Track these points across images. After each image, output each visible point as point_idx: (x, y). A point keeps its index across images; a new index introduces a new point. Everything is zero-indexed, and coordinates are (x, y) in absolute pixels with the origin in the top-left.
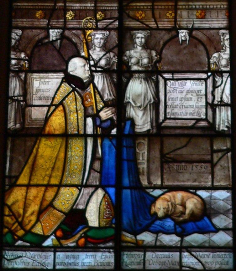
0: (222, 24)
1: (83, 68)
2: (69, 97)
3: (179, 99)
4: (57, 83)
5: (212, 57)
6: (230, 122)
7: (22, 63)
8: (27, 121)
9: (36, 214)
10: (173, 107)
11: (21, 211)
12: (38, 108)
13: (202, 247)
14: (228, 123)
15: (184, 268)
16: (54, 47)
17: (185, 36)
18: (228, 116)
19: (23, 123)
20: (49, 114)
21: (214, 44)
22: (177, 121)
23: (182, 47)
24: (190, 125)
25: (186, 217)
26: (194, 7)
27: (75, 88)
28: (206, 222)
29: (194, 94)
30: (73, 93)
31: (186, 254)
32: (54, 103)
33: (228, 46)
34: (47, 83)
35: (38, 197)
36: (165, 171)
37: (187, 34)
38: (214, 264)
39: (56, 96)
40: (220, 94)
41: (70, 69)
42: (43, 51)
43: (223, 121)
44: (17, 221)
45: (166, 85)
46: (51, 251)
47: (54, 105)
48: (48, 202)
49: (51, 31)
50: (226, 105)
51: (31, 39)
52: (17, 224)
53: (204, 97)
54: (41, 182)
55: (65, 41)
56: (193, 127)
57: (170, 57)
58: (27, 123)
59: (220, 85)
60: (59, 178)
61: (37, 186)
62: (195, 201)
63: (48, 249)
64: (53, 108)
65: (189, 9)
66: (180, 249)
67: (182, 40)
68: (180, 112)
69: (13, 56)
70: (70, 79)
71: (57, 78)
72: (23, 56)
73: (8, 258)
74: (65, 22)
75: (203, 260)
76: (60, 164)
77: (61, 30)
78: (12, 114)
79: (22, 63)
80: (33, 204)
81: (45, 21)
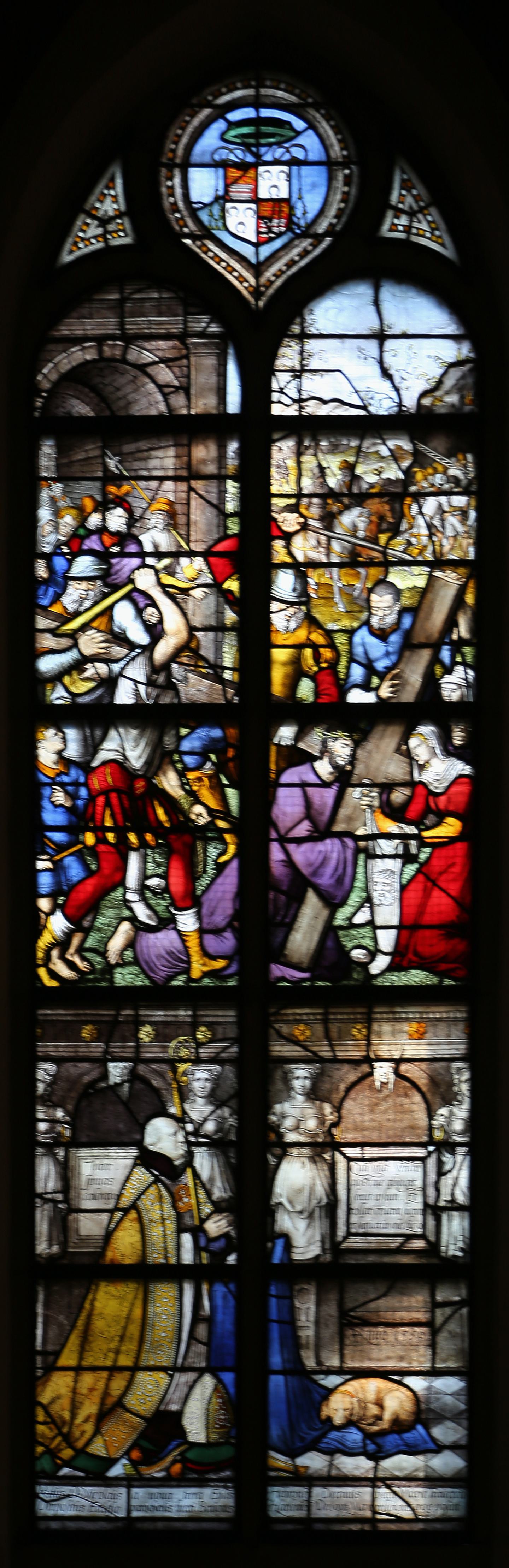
4: (126, 1167)
7: (59, 1128)
9: (92, 1420)
10: (363, 1212)
11: (67, 1415)
15: (379, 1516)
16: (119, 1097)
22: (371, 1239)
23: (381, 1095)
24: (393, 1246)
25: (385, 1425)
29: (402, 1188)
31: (384, 1490)
33: (467, 1093)
36: (347, 1342)
37: (391, 1070)
41: (149, 1140)
44: (60, 1433)
45: (349, 1169)
48: (114, 1399)
50: (460, 1208)
52: (59, 1439)
53: (420, 1193)
54: (100, 1363)
55: (139, 1086)
56: (399, 1251)
58: (71, 1244)
59: (450, 1171)
60: (133, 1355)
61: (94, 1369)
64: (118, 1215)
66: (373, 1482)
68: (374, 1222)
71: (125, 1158)
72: (60, 1114)
74: (138, 1047)
76: (134, 1330)
79: (59, 1128)
80: (87, 1403)
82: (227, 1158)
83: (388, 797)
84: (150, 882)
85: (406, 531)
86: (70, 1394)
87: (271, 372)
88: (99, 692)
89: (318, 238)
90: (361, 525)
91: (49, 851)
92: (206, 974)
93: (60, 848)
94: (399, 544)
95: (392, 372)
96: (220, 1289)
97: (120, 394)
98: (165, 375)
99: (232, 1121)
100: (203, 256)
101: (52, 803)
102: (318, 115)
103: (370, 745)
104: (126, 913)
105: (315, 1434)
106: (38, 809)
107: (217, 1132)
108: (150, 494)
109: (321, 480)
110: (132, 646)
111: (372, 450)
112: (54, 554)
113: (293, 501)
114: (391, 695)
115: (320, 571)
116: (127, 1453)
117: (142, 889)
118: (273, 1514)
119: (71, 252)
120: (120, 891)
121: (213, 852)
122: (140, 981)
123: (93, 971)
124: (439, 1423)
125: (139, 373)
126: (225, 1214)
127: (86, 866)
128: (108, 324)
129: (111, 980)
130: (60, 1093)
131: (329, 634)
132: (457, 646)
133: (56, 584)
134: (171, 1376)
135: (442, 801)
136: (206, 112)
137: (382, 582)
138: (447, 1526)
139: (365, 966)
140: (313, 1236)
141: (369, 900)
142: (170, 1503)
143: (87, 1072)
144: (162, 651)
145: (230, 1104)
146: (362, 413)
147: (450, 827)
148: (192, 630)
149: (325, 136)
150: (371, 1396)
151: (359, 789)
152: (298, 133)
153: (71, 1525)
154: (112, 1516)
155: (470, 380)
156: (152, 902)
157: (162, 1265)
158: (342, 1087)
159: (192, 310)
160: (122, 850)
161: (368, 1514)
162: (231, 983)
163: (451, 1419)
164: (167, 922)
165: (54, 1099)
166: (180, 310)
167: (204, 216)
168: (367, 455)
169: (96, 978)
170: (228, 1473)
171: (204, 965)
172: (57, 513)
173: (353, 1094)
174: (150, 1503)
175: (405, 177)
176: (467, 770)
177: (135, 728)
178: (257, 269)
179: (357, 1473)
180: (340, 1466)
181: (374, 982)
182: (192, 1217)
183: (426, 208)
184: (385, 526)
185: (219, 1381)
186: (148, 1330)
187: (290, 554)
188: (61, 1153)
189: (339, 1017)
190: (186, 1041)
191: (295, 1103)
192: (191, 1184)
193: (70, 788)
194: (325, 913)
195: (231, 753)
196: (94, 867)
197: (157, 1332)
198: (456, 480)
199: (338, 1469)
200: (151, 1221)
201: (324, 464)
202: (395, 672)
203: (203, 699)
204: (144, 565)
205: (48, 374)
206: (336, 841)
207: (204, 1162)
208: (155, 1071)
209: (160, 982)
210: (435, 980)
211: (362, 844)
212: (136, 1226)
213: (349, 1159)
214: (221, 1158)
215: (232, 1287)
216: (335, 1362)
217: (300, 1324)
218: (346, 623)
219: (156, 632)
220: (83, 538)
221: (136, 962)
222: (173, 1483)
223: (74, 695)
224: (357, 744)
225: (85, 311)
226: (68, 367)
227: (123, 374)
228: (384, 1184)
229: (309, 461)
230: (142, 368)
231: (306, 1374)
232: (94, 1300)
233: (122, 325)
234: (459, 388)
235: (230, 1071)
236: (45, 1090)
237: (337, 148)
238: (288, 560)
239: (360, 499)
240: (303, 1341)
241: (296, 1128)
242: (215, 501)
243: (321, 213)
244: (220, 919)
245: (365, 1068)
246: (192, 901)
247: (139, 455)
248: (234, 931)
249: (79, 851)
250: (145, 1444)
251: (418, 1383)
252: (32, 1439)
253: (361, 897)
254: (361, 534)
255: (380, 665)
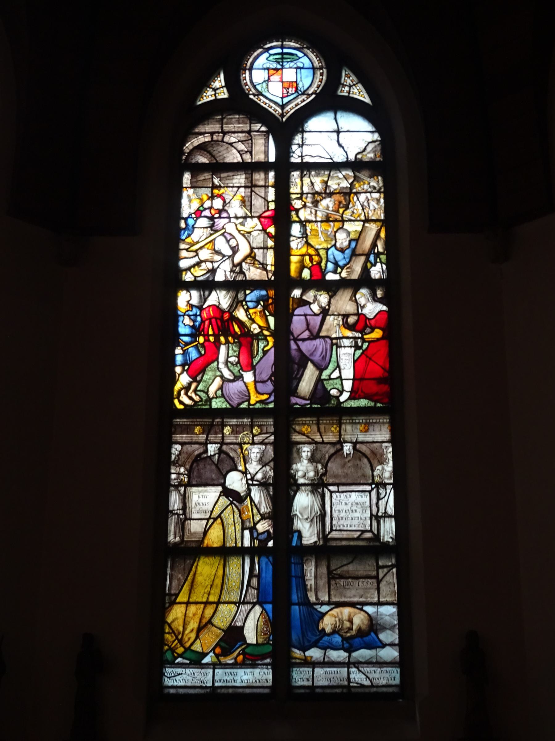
0: (385, 437)
1: (240, 481)
2: (227, 510)
3: (344, 511)
4: (215, 497)
5: (375, 469)
6: (394, 533)
7: (182, 477)
8: (186, 534)
9: (195, 631)
10: (339, 519)
11: (181, 629)
12: (197, 521)
13: (368, 663)
14: (392, 534)
15: (351, 684)
17: (349, 449)
18: (392, 527)
19: (182, 537)
20: (208, 527)
21: (378, 457)
23: (347, 460)
24: (355, 536)
25: (353, 632)
26: (357, 421)
27: (233, 501)
28: (373, 637)
29: (359, 506)
30: (231, 506)
31: (354, 670)
32: (213, 516)
34: (205, 497)
35: (197, 614)
36: (332, 587)
37: (351, 447)
38: (382, 679)
39: (214, 509)
40: (384, 506)
41: (227, 484)
42: (201, 465)
43: (387, 532)
44: (177, 638)
46: (210, 668)
47: (213, 518)
48: (207, 620)
49: (209, 446)
50: (390, 516)
51: (189, 455)
52: (176, 641)
54: (200, 600)
55: (223, 456)
56: (358, 539)
57: (335, 470)
58: (186, 536)
59: (384, 497)
61: (196, 603)
62: (362, 617)
63: (207, 666)
64: (211, 521)
65: (353, 423)
66: (348, 664)
67: (346, 454)
68: (346, 524)
69: (173, 471)
70: (227, 492)
72: (182, 470)
73: (168, 676)
74: (223, 437)
75: (371, 676)
76: (218, 582)
77: (219, 445)
78: (172, 528)
79: (182, 477)
80: (192, 621)
81: (204, 437)
82: (268, 491)
83: (347, 320)
84: (230, 359)
85: (351, 208)
86: (183, 617)
87: (290, 144)
88: (208, 275)
89: (309, 95)
90: (331, 205)
91: (181, 345)
92: (257, 402)
93: (187, 344)
94: (348, 212)
95: (343, 145)
96: (264, 560)
97: (220, 154)
98: (241, 147)
99: (271, 473)
100: (259, 102)
101: (184, 324)
102: (308, 51)
103: (337, 297)
104: (218, 373)
105: (315, 638)
106: (177, 326)
107: (262, 479)
108: (234, 194)
109: (312, 187)
110: (224, 256)
111: (335, 175)
112: (189, 217)
113: (299, 196)
114: (346, 276)
115: (313, 224)
116: (214, 649)
117: (227, 362)
118: (294, 684)
119: (200, 101)
120: (215, 364)
121: (261, 345)
122: (225, 405)
123: (201, 400)
124: (383, 632)
125: (229, 146)
126: (267, 520)
127: (199, 352)
128: (216, 127)
129: (210, 405)
130: (183, 460)
131: (317, 250)
132: (378, 255)
133: (189, 230)
134: (238, 607)
135: (373, 322)
136: (260, 50)
137: (342, 228)
138: (390, 690)
139: (337, 398)
140: (313, 531)
141: (338, 366)
142: (236, 678)
143: (197, 450)
144: (238, 258)
145: (269, 464)
146: (331, 161)
147: (377, 334)
148: (252, 249)
149: (311, 59)
150: (345, 617)
151: (332, 317)
152: (300, 58)
153: (181, 691)
154: (204, 685)
155: (379, 148)
156: (232, 368)
157: (233, 547)
158: (327, 456)
159: (253, 122)
160: (217, 344)
161: (346, 683)
162: (271, 406)
163: (390, 629)
164: (238, 378)
165: (180, 462)
166: (248, 122)
167: (259, 87)
168: (333, 177)
169: (202, 404)
170: (268, 661)
171: (257, 397)
172: (190, 201)
173: (332, 460)
174: (225, 678)
175: (347, 73)
176: (385, 308)
177: (225, 290)
178: (283, 107)
179: (339, 660)
180: (330, 656)
181: (342, 405)
182: (250, 522)
183: (357, 84)
184: (341, 205)
185: (264, 609)
186: (226, 582)
187: (298, 216)
188: (182, 489)
189: (325, 422)
190: (247, 434)
191: (303, 464)
192: (249, 505)
193: (192, 317)
194: (317, 373)
195: (270, 301)
196: (203, 352)
197: (230, 583)
198: (374, 188)
199: (329, 658)
200: (228, 524)
201: (313, 181)
202: (348, 266)
203: (257, 278)
204: (230, 222)
205: (188, 146)
206: (322, 340)
207: (257, 494)
208: (231, 448)
209: (235, 406)
210: (373, 404)
211: (334, 341)
212: (221, 527)
213: (331, 492)
214: (265, 492)
215: (271, 558)
216: (326, 599)
217: (306, 578)
218: (325, 245)
219: (235, 250)
220: (202, 211)
221: (223, 396)
222: (239, 666)
223: (195, 277)
224: (331, 297)
225: (206, 123)
226: (198, 144)
227: (222, 146)
228: (350, 505)
229: (306, 180)
230: (231, 144)
231: (312, 605)
232: (197, 565)
233: (222, 128)
234: (374, 151)
235: (270, 449)
236: (175, 458)
237: (317, 63)
238: (297, 219)
239: (331, 195)
240: (309, 587)
241: (304, 476)
242: (263, 196)
243: (311, 85)
244: (265, 376)
245: (338, 446)
246: (252, 367)
247: (229, 178)
248: (271, 381)
249: (196, 345)
250: (223, 644)
251: (370, 609)
252: (163, 642)
253: (334, 365)
254: (331, 209)
255: (341, 263)
